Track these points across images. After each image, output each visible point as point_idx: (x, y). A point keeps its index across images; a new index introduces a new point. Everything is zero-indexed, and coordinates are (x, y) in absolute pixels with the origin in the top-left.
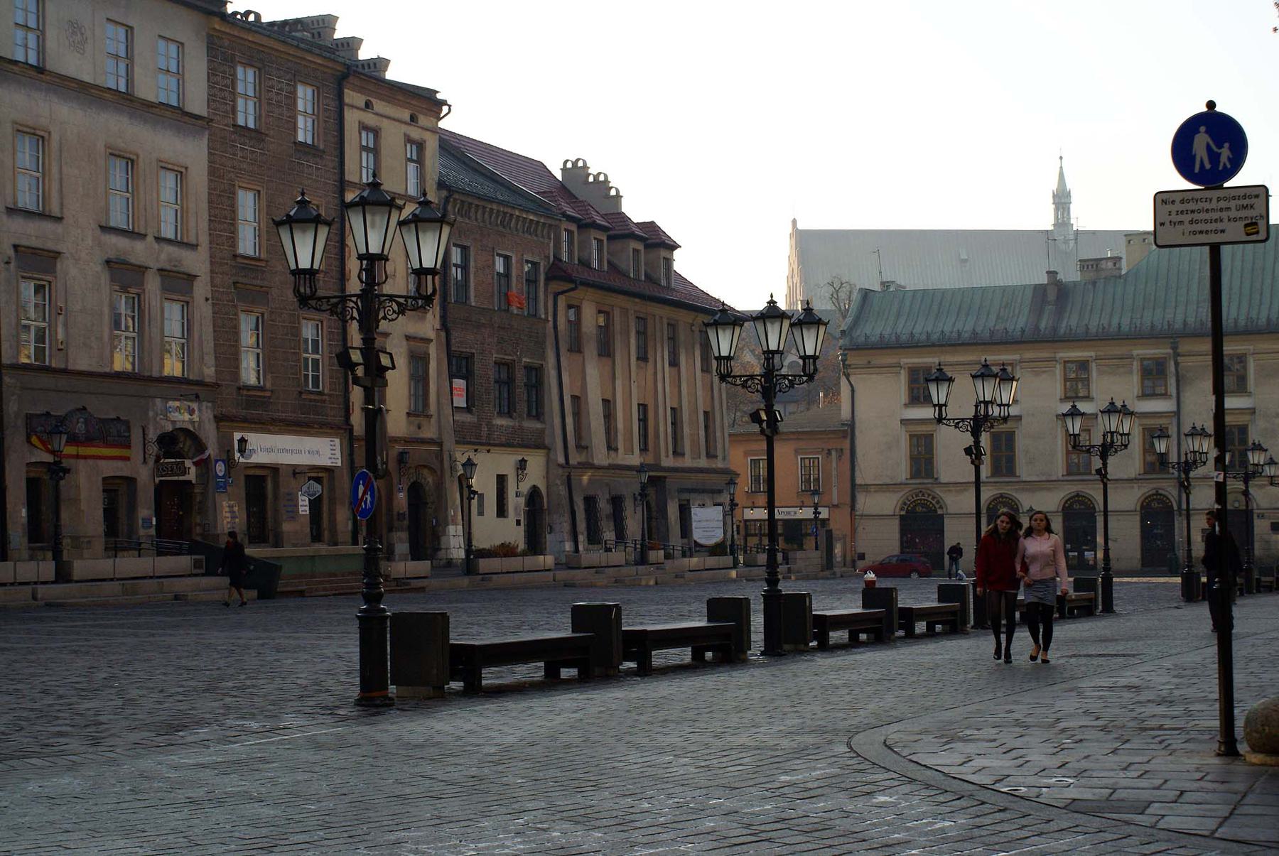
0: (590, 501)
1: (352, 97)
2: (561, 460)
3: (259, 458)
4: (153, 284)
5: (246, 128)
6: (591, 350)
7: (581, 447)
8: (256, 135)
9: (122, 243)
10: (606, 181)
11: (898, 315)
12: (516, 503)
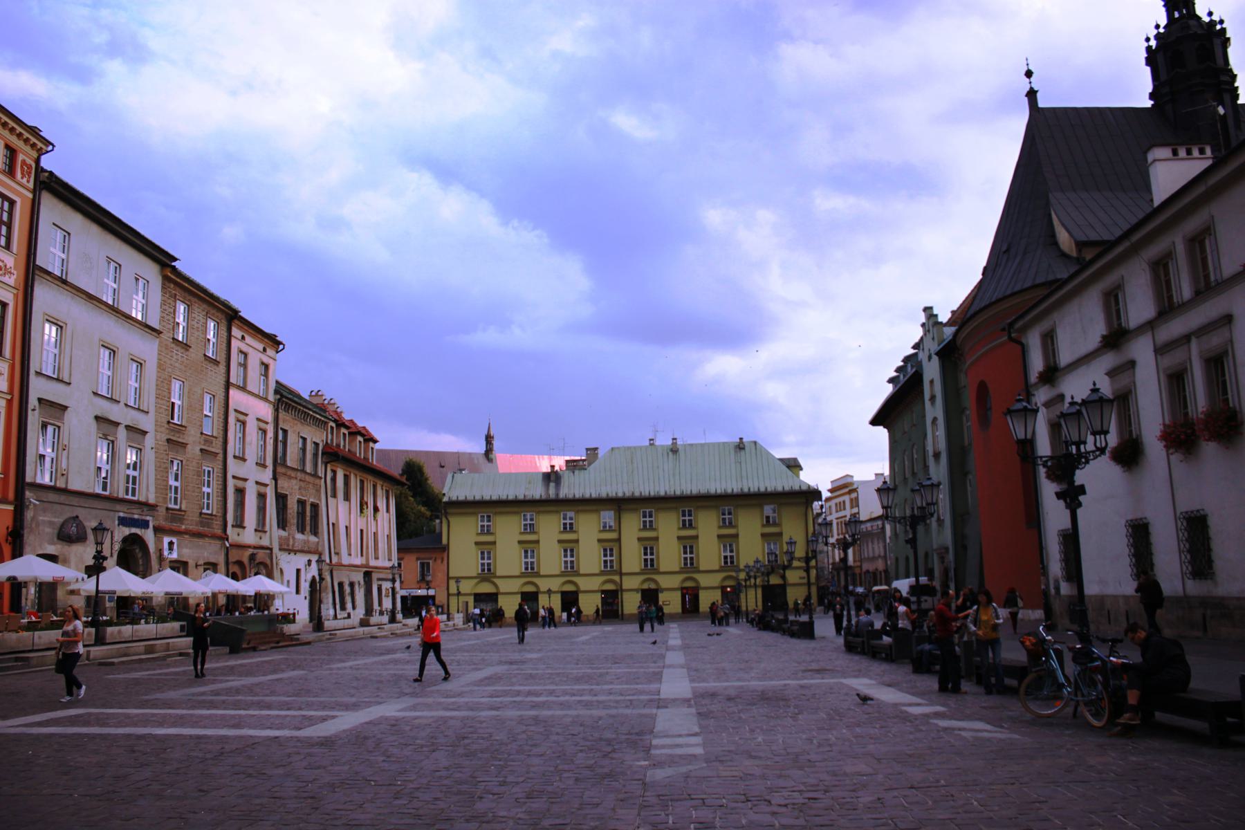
0: (341, 585)
1: (236, 332)
4: (122, 433)
8: (186, 346)
12: (305, 586)
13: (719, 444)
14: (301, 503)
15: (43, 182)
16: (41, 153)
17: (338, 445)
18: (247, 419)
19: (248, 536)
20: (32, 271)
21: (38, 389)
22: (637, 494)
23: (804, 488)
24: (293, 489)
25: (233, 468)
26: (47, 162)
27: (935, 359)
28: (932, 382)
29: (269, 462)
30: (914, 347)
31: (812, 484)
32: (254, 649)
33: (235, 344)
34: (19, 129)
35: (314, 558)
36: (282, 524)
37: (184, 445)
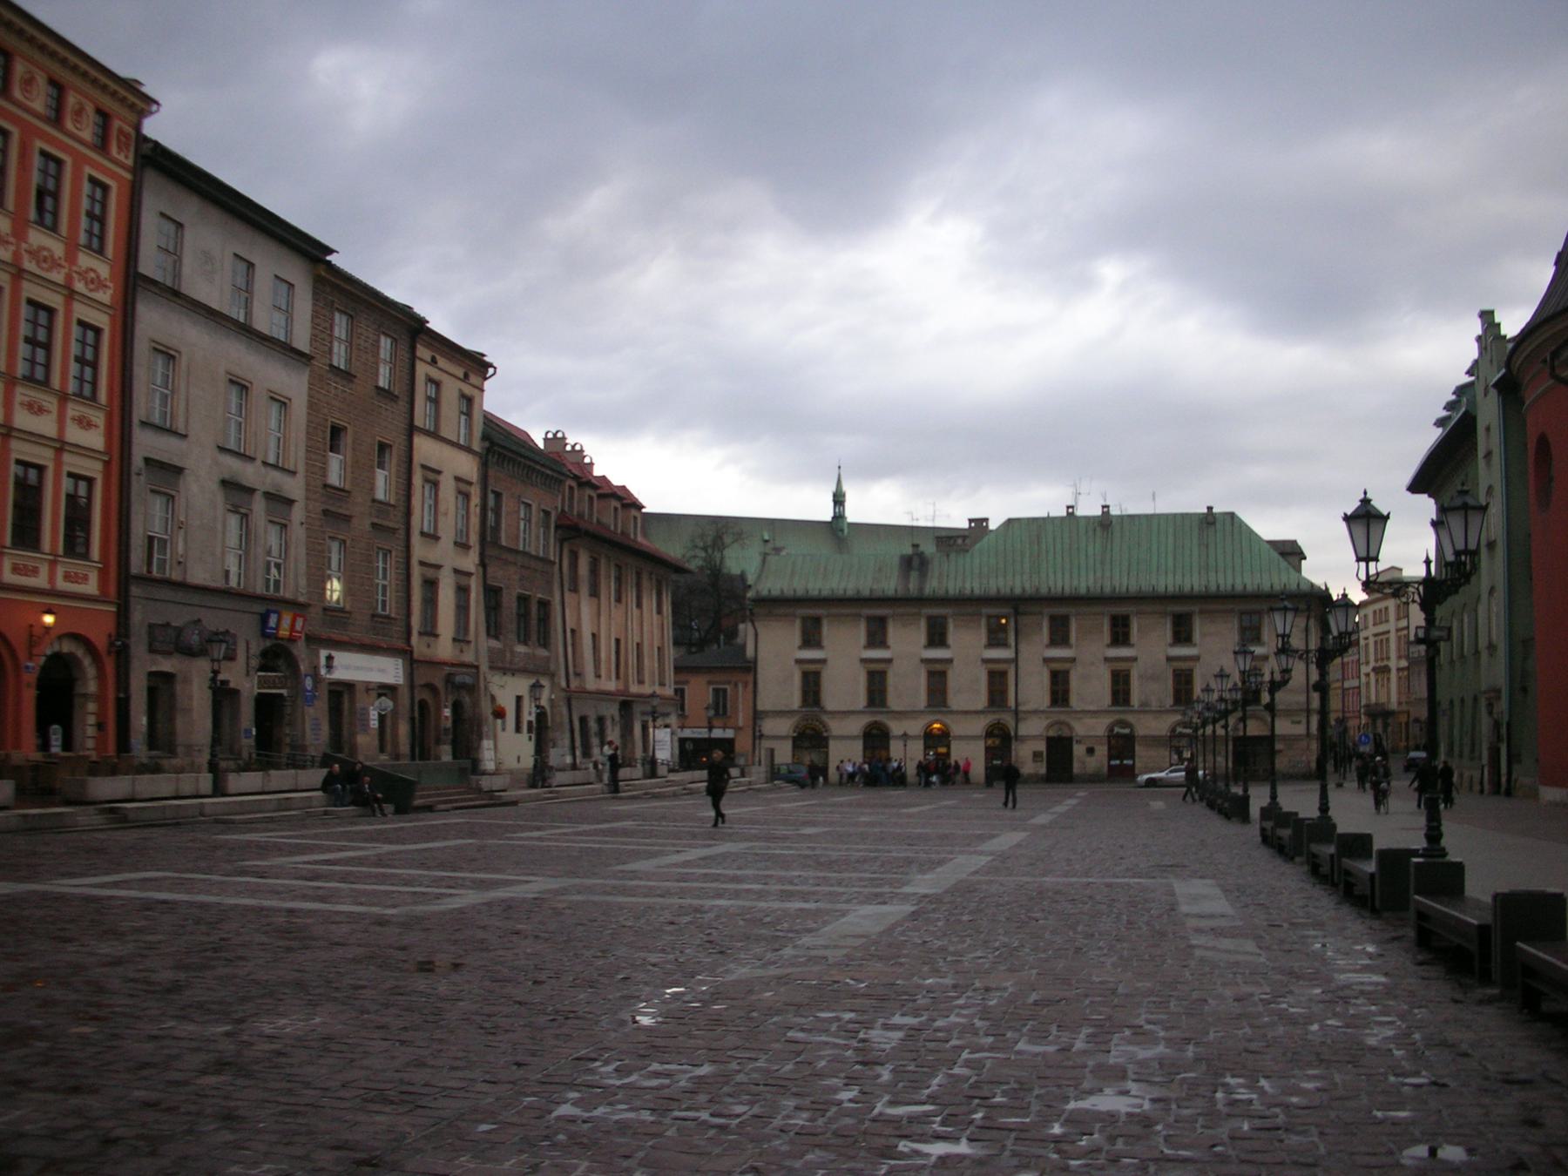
0: (583, 720)
1: (423, 352)
2: (564, 684)
3: (339, 674)
4: (259, 506)
5: (338, 368)
6: (584, 589)
7: (578, 675)
8: (347, 376)
9: (233, 465)
10: (582, 451)
11: (793, 574)
13: (1175, 515)
14: (523, 600)
15: (144, 157)
16: (142, 114)
17: (581, 516)
18: (442, 478)
19: (444, 648)
20: (133, 283)
21: (145, 444)
22: (1044, 591)
23: (1304, 587)
24: (512, 583)
25: (419, 550)
26: (153, 128)
27: (1493, 393)
28: (1488, 429)
29: (474, 539)
30: (1469, 373)
31: (1318, 581)
32: (429, 808)
33: (422, 370)
34: (113, 86)
35: (545, 682)
36: (494, 630)
37: (347, 519)
